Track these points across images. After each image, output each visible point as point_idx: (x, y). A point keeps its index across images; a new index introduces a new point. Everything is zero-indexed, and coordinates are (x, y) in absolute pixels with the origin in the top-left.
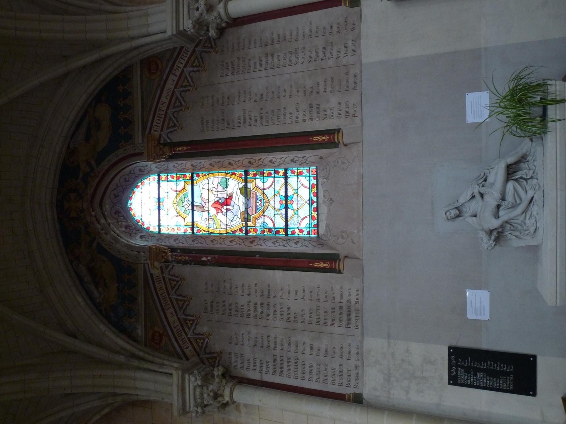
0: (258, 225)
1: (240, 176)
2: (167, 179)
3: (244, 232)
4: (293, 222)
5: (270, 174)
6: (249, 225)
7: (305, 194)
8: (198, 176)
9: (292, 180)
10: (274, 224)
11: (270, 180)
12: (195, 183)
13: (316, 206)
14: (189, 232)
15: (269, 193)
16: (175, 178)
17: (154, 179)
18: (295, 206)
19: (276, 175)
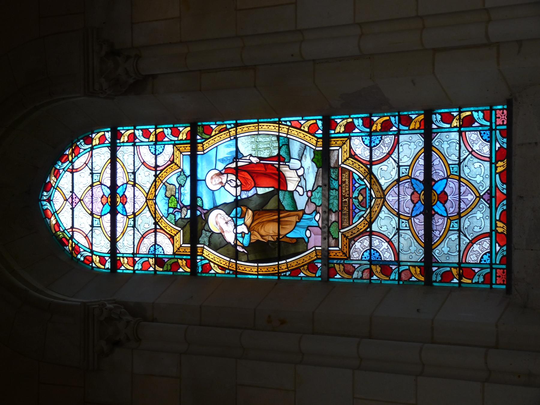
0: (355, 256)
1: (312, 131)
2: (132, 139)
3: (319, 273)
4: (446, 250)
5: (386, 127)
10: (397, 254)
11: (389, 140)
12: (200, 148)
15: (385, 174)
16: (152, 138)
17: (102, 140)
19: (402, 127)
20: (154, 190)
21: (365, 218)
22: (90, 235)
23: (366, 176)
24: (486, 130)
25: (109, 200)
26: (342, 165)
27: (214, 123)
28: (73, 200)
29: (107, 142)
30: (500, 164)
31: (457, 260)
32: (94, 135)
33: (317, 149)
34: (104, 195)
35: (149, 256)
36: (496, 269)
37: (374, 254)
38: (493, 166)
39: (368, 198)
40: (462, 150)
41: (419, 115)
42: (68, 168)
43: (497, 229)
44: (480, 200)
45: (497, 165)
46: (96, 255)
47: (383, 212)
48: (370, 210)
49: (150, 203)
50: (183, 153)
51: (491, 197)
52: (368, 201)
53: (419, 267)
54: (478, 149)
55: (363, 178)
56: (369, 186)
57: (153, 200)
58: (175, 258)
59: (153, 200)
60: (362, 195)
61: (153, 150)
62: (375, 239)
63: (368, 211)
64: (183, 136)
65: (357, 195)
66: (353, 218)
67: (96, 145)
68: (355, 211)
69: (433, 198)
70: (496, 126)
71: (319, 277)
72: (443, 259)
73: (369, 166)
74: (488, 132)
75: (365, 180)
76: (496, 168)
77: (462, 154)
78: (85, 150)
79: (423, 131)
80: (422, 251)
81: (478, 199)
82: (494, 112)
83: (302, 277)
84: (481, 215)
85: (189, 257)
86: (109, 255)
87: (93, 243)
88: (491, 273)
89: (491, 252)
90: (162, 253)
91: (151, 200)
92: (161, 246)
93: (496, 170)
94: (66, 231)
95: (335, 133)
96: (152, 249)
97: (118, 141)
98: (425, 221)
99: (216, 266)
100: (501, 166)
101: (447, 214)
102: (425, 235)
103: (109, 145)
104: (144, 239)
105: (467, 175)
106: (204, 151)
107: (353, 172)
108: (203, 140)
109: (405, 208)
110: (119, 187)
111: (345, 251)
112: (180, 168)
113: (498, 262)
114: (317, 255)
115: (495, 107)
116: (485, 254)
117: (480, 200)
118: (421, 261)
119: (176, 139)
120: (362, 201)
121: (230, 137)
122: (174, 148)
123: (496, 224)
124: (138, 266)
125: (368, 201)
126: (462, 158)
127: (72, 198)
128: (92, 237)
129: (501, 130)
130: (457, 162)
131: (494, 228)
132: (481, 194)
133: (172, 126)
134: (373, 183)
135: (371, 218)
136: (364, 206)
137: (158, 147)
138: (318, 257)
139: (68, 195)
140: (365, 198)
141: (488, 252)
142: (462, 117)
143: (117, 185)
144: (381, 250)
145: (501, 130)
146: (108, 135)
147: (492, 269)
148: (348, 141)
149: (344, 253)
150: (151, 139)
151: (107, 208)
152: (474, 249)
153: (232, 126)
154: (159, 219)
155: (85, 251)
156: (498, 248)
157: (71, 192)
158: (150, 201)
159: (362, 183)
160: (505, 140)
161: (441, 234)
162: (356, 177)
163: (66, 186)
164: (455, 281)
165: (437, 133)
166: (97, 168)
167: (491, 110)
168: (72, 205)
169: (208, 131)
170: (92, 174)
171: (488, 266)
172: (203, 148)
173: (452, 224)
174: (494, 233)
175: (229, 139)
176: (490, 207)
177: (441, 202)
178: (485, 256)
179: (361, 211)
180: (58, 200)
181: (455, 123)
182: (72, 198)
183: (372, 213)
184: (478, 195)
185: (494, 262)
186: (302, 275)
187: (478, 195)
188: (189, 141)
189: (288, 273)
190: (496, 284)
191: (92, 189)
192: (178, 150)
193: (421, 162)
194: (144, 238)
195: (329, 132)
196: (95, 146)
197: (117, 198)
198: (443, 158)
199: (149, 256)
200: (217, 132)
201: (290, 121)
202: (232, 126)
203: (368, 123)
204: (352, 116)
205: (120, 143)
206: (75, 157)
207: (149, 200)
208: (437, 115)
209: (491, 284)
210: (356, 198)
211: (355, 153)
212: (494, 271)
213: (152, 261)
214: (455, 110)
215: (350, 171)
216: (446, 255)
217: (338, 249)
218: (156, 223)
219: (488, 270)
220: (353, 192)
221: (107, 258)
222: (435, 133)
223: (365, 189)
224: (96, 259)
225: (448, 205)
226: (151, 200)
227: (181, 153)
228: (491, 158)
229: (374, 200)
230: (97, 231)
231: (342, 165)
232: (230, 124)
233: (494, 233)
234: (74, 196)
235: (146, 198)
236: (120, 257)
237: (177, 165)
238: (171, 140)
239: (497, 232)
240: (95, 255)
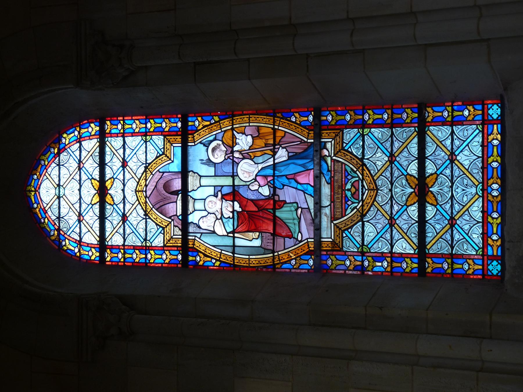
20: (144, 180)
21: (358, 210)
23: (359, 168)
33: (309, 141)
48: (363, 203)
49: (139, 194)
50: (174, 145)
55: (355, 170)
56: (361, 177)
57: (143, 191)
59: (143, 191)
60: (355, 187)
63: (361, 203)
65: (350, 187)
66: (346, 210)
75: (357, 172)
91: (140, 191)
104: (138, 231)
106: (194, 142)
108: (194, 132)
112: (170, 159)
120: (355, 193)
122: (164, 139)
136: (357, 198)
138: (310, 249)
140: (357, 190)
148: (341, 133)
154: (149, 210)
158: (140, 193)
162: (349, 170)
172: (194, 139)
179: (353, 203)
192: (169, 141)
197: (104, 190)
207: (138, 191)
210: (349, 190)
215: (342, 163)
218: (146, 215)
220: (346, 184)
223: (358, 181)
226: (140, 191)
227: (172, 145)
229: (367, 191)
237: (168, 157)
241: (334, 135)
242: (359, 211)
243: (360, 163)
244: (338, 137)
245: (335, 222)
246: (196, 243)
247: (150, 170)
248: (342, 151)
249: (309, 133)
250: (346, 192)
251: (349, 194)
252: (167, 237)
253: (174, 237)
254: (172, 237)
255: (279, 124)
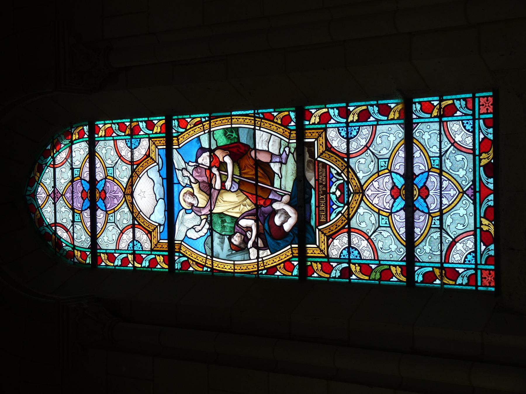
3: (295, 272)
5: (364, 116)
6: (310, 253)
7: (461, 168)
8: (183, 124)
9: (427, 133)
13: (491, 203)
14: (162, 266)
15: (363, 167)
18: (433, 202)
21: (343, 214)
22: (71, 230)
23: (344, 170)
24: (469, 120)
25: (89, 195)
26: (319, 159)
27: (188, 116)
28: (55, 196)
29: (86, 136)
30: (484, 155)
31: (438, 260)
32: (73, 130)
34: (84, 189)
35: (127, 252)
36: (481, 269)
37: (353, 252)
38: (477, 158)
39: (346, 193)
40: (443, 143)
41: (397, 104)
42: (50, 164)
43: (482, 227)
44: (463, 195)
45: (481, 157)
46: (78, 250)
47: (361, 208)
50: (159, 147)
51: (475, 192)
52: (346, 196)
53: (400, 266)
54: (461, 140)
55: (340, 172)
56: (346, 179)
58: (151, 254)
60: (339, 190)
61: (129, 145)
62: (354, 236)
63: (346, 207)
64: (157, 129)
65: (334, 191)
66: (330, 215)
67: (76, 140)
68: (333, 207)
69: (415, 193)
70: (480, 114)
71: (295, 276)
72: (425, 258)
73: (346, 160)
74: (471, 122)
75: (342, 174)
76: (480, 160)
77: (443, 146)
78: (65, 145)
79: (402, 121)
80: (403, 250)
81: (461, 194)
82: (477, 100)
83: (278, 276)
84: (465, 212)
85: (166, 253)
86: (90, 250)
87: (75, 237)
88: (476, 274)
89: (475, 252)
90: (141, 249)
92: (139, 242)
93: (480, 162)
94: (49, 226)
95: (309, 124)
96: (131, 245)
97: (96, 136)
98: (406, 218)
99: (194, 263)
100: (486, 159)
101: (429, 211)
102: (406, 232)
103: (87, 139)
105: (449, 169)
106: (179, 145)
107: (330, 166)
109: (385, 204)
110: (99, 182)
111: (322, 248)
112: (155, 162)
113: (483, 262)
114: (292, 253)
115: (477, 95)
116: (470, 254)
117: (463, 195)
118: (401, 261)
119: (151, 132)
120: (340, 196)
121: (204, 131)
123: (481, 222)
124: (118, 262)
125: (346, 196)
126: (443, 150)
127: (55, 194)
128: (73, 233)
129: (484, 119)
130: (438, 155)
131: (478, 226)
132: (464, 190)
133: (146, 119)
134: (350, 177)
135: (349, 214)
137: (133, 140)
139: (51, 190)
141: (472, 252)
142: (443, 106)
143: (97, 180)
144: (360, 248)
145: (484, 119)
146: (86, 128)
147: (476, 269)
148: (324, 133)
149: (321, 251)
150: (127, 132)
151: (87, 204)
152: (458, 249)
153: (207, 119)
154: (137, 214)
155: (67, 245)
156: (483, 248)
157: (53, 187)
159: (341, 178)
160: (491, 130)
161: (422, 232)
162: (334, 172)
163: (48, 181)
164: (438, 282)
165: (418, 123)
166: (77, 163)
167: (474, 98)
168: (54, 201)
169: (183, 124)
170: (72, 169)
171: (473, 266)
172: (178, 142)
173: (434, 221)
174: (478, 230)
175: (203, 133)
176: (474, 203)
177: (422, 198)
178: (469, 256)
179: (339, 207)
180: (41, 194)
181: (435, 113)
182: (55, 194)
183: (351, 209)
184: (461, 191)
185: (479, 262)
186: (278, 273)
187: (461, 191)
188: (164, 135)
189: (264, 272)
190: (481, 286)
191: (72, 184)
193: (402, 154)
194: (123, 233)
195: (303, 122)
196: (75, 140)
198: (424, 149)
199: (127, 252)
200: (192, 126)
201: (262, 113)
202: (207, 119)
203: (345, 113)
204: (328, 106)
205: (98, 137)
206: (56, 152)
208: (417, 104)
209: (477, 286)
210: (334, 193)
211: (331, 145)
212: (479, 272)
213: (130, 257)
214: (127, 120)
216: (428, 255)
217: (315, 246)
219: (473, 272)
220: (330, 188)
221: (88, 253)
222: (415, 123)
223: (343, 184)
224: (78, 254)
225: (429, 200)
227: (156, 147)
228: (474, 149)
229: (352, 195)
230: (78, 227)
231: (319, 159)
232: (204, 117)
233: (478, 230)
234: (56, 191)
235: (124, 193)
236: (100, 253)
237: (153, 160)
238: (146, 134)
239: (481, 229)
240: (77, 250)
241: (317, 135)
242: (344, 216)
243: (346, 165)
244: (321, 138)
245: (320, 227)
246: (182, 248)
247: (137, 173)
248: (326, 152)
249: (290, 134)
250: (331, 195)
251: (333, 197)
252: (154, 241)
253: (161, 241)
254: (158, 242)
255: (260, 125)
